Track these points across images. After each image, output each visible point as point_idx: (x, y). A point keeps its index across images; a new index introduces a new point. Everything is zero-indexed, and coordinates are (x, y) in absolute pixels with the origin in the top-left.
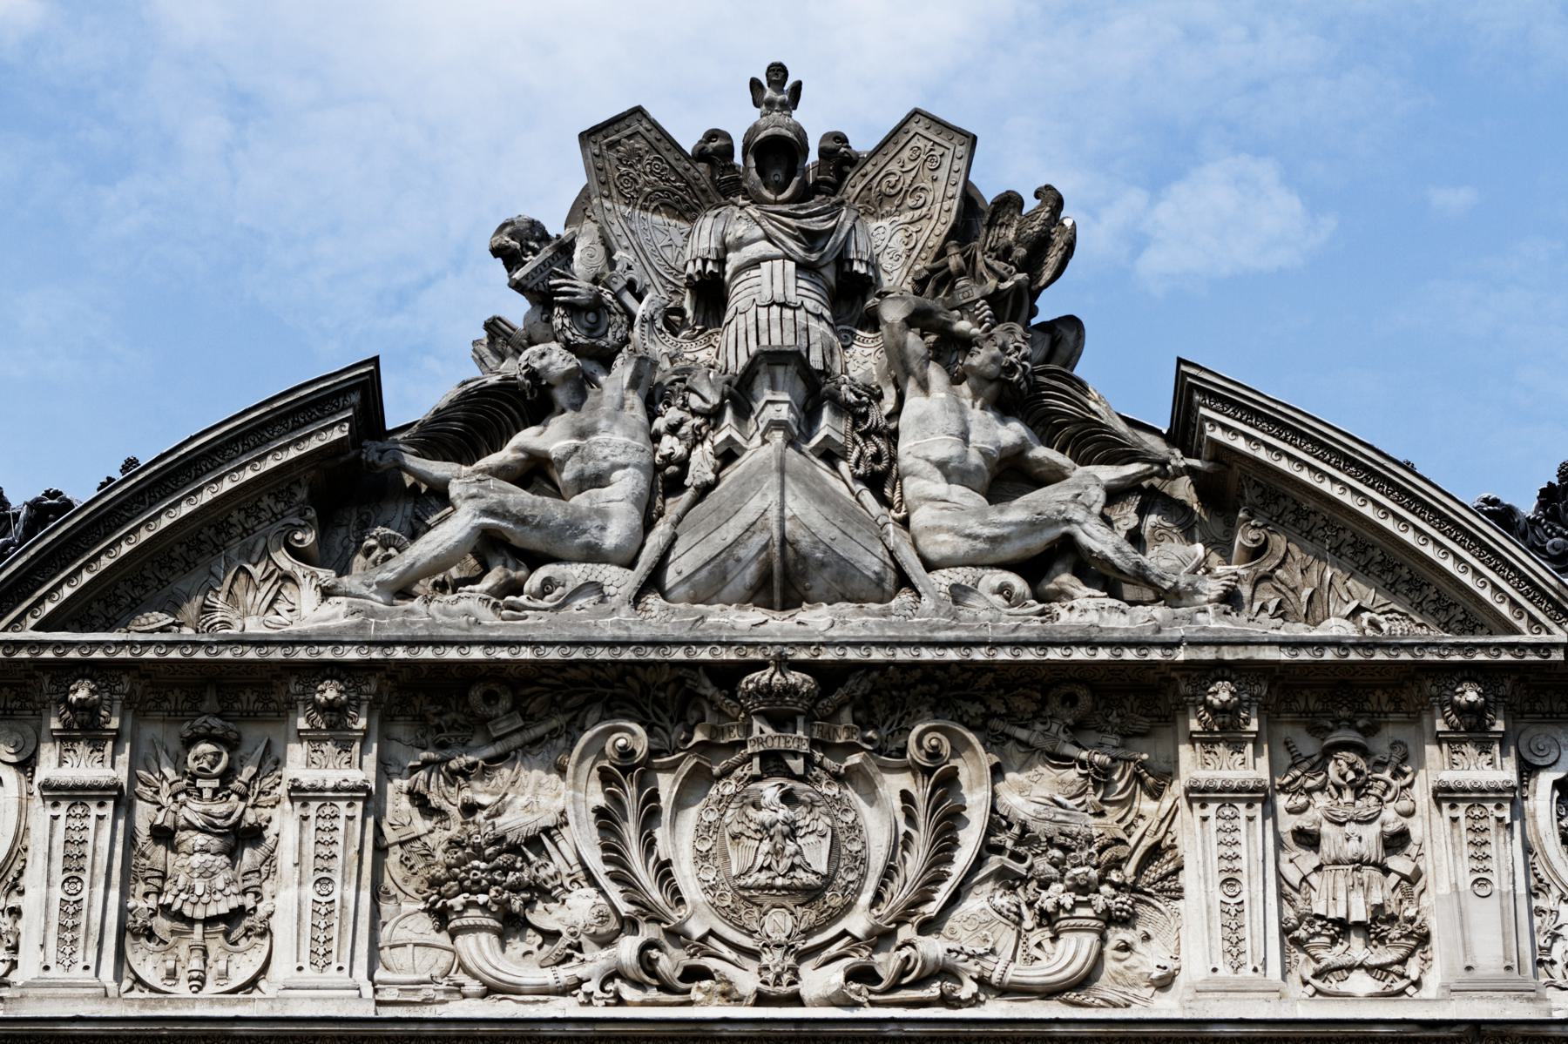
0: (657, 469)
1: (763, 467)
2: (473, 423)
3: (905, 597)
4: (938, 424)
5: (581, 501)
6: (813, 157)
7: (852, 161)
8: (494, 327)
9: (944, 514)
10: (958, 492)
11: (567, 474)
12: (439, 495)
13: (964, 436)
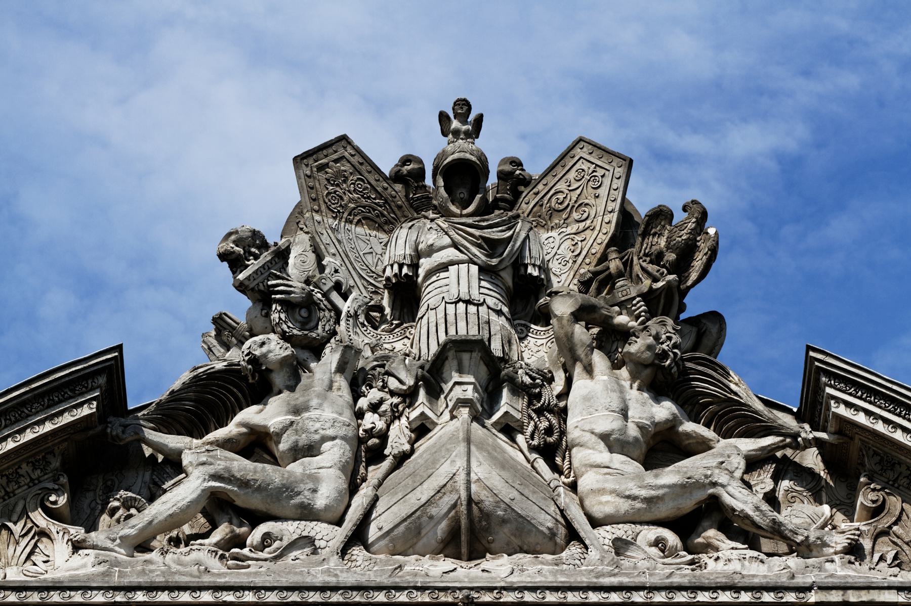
0: (361, 441)
1: (452, 438)
2: (203, 403)
3: (575, 549)
4: (601, 401)
5: (296, 468)
6: (493, 180)
7: (526, 182)
8: (220, 322)
9: (606, 478)
10: (618, 460)
11: (284, 446)
12: (174, 465)
13: (624, 413)
